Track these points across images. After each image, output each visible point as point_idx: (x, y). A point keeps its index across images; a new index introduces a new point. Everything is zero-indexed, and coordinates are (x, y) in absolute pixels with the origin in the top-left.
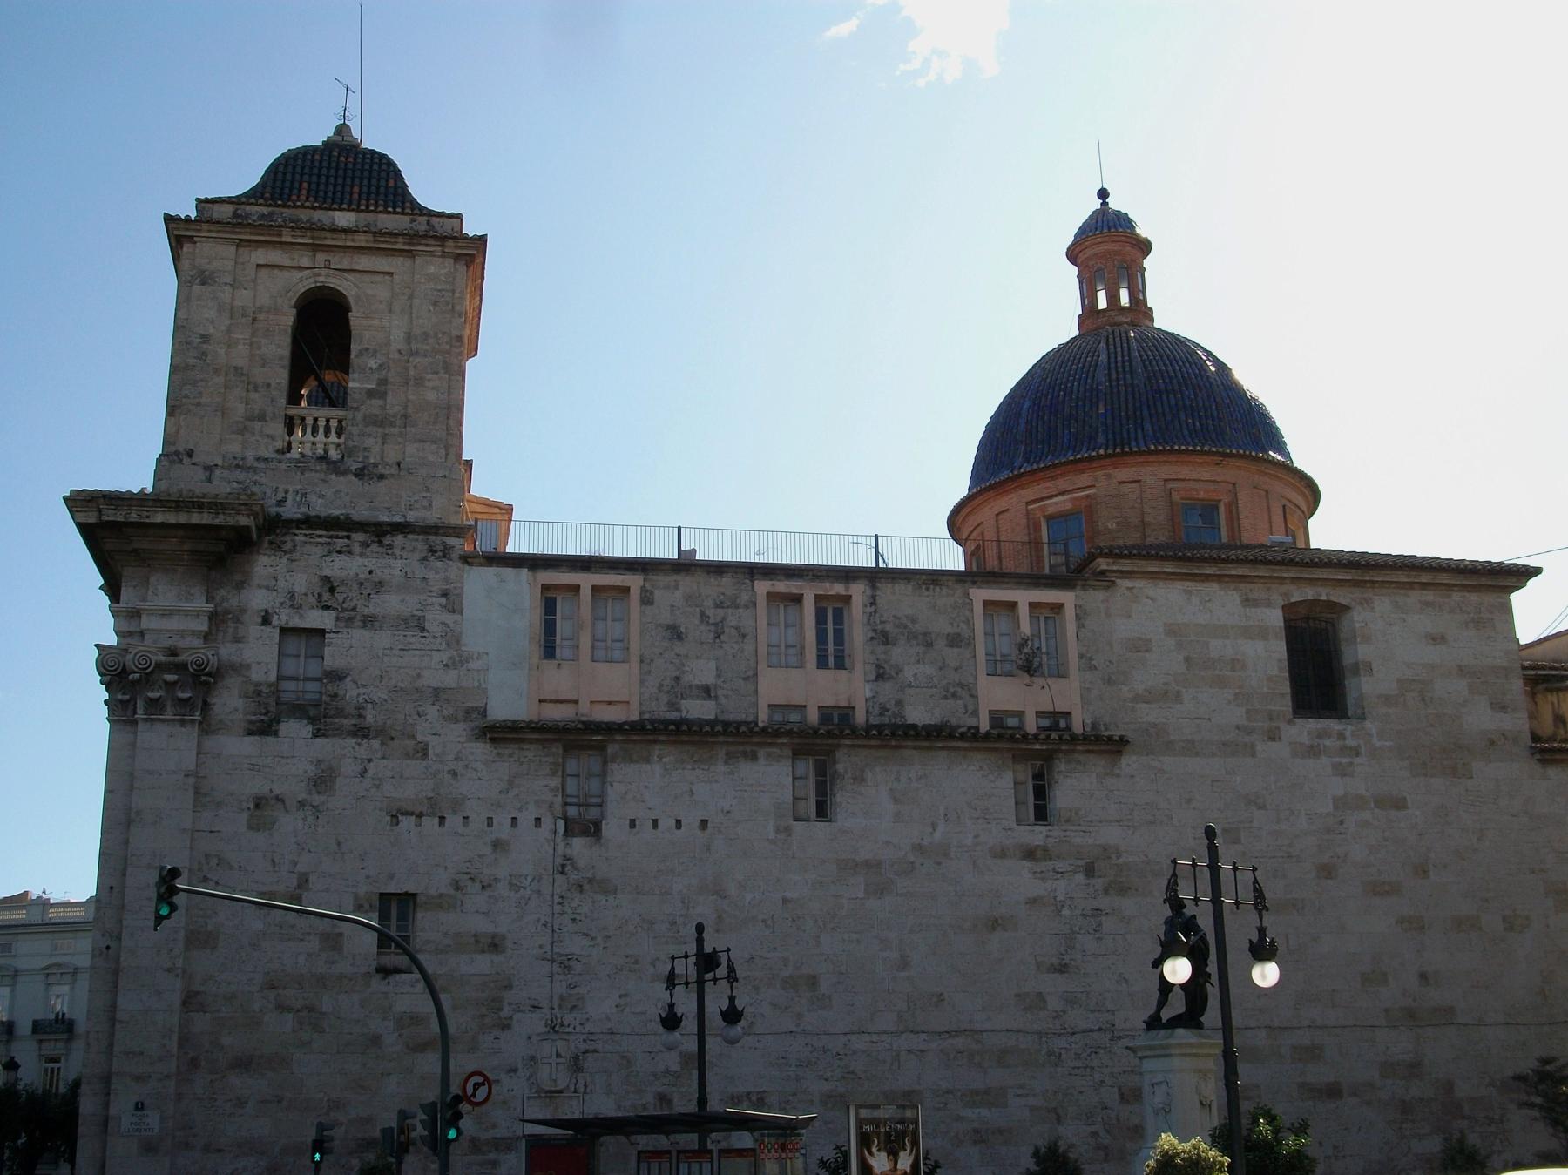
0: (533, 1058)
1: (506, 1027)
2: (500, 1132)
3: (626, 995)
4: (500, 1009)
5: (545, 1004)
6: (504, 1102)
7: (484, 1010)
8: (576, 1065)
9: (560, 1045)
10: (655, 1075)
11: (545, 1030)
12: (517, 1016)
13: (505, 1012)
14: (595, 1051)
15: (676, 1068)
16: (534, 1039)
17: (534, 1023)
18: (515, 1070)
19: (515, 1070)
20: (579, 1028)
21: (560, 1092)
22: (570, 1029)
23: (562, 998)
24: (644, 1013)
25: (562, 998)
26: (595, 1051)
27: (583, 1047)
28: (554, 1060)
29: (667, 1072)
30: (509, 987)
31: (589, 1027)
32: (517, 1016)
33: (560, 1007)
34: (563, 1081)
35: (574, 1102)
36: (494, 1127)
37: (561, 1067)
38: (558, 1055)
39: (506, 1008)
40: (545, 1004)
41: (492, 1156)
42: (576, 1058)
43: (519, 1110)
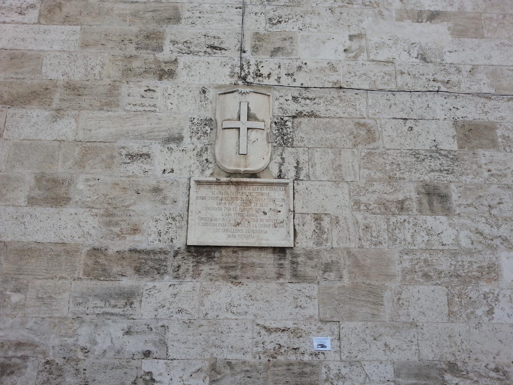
0: (209, 122)
1: (166, 73)
2: (145, 241)
3: (360, 36)
4: (160, 49)
5: (231, 43)
6: (156, 190)
7: (131, 50)
8: (282, 134)
9: (257, 103)
10: (416, 154)
11: (228, 81)
12: (183, 60)
13: (167, 53)
14: (312, 115)
15: (450, 144)
16: (211, 94)
17: (218, 71)
18: (179, 139)
19: (179, 139)
20: (285, 81)
21: (254, 175)
22: (272, 81)
23: (258, 37)
24: (390, 62)
25: (258, 37)
26: (312, 115)
27: (293, 108)
28: (244, 124)
29: (436, 151)
30: (175, 18)
31: (301, 78)
32: (183, 60)
33: (255, 49)
34: (259, 155)
35: (278, 194)
36: (135, 230)
37: (253, 135)
38: (250, 117)
39: (167, 47)
40: (231, 43)
41: (126, 283)
42: (281, 124)
43: (181, 204)
